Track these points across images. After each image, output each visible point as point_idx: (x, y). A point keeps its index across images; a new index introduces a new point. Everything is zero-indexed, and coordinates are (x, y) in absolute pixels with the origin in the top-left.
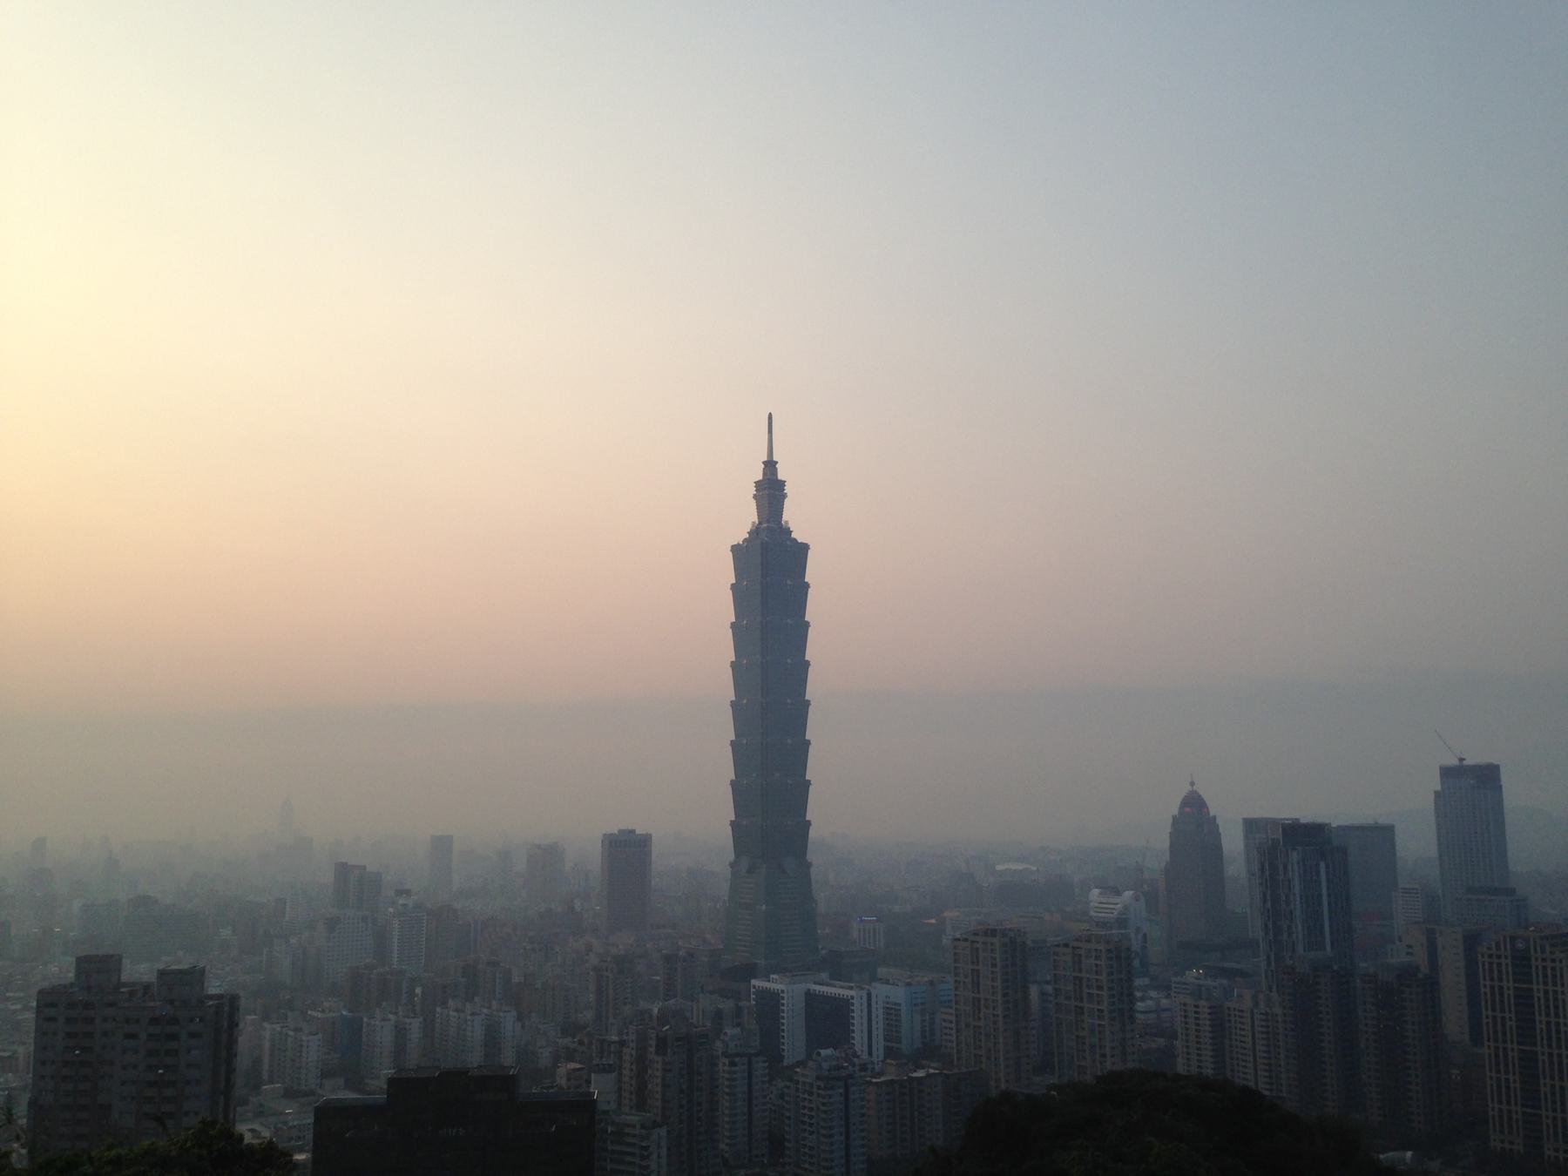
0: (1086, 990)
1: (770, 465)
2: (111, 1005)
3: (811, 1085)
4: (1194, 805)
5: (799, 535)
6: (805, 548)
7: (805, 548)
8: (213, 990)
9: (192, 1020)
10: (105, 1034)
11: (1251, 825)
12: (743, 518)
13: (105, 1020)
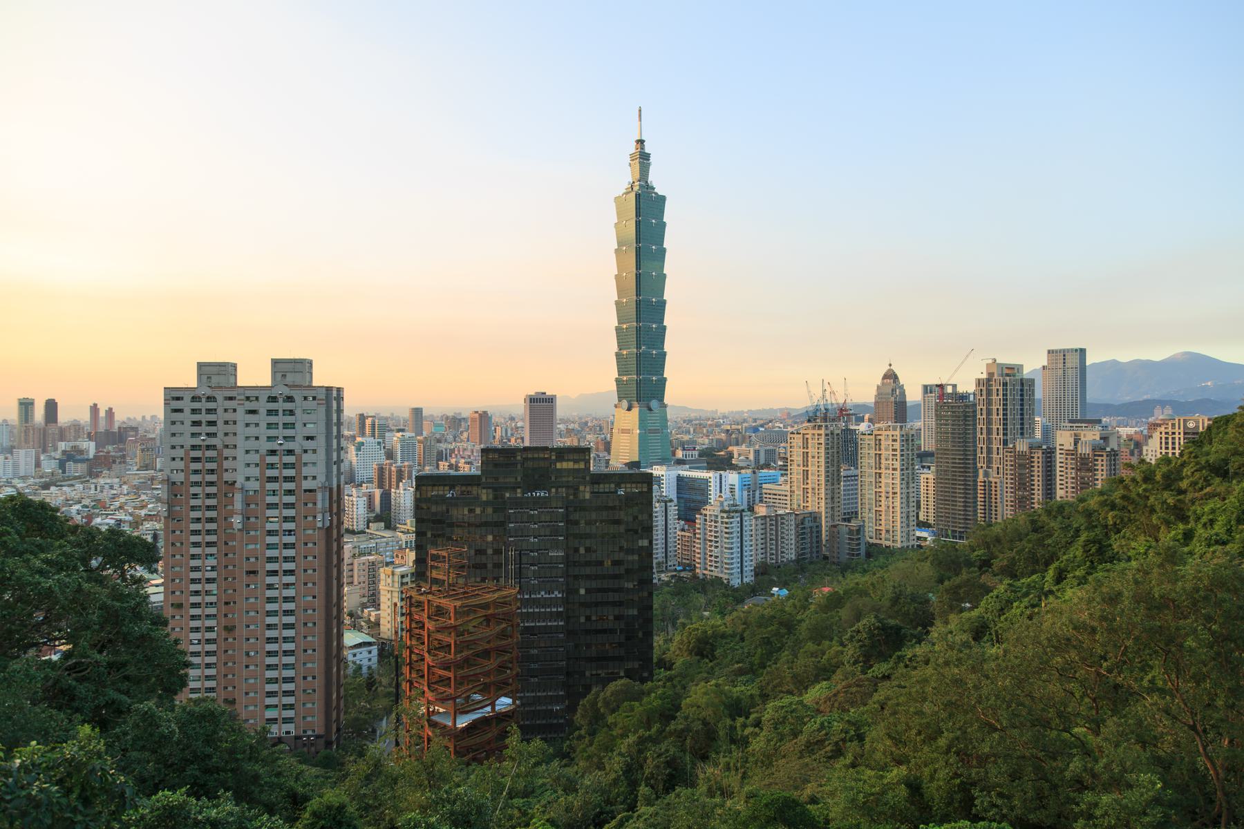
0: (883, 461)
1: (641, 142)
2: (231, 399)
3: (716, 516)
4: (891, 376)
5: (660, 191)
6: (663, 199)
7: (663, 199)
8: (317, 381)
9: (305, 398)
10: (226, 423)
11: (927, 389)
12: (623, 178)
13: (226, 410)
